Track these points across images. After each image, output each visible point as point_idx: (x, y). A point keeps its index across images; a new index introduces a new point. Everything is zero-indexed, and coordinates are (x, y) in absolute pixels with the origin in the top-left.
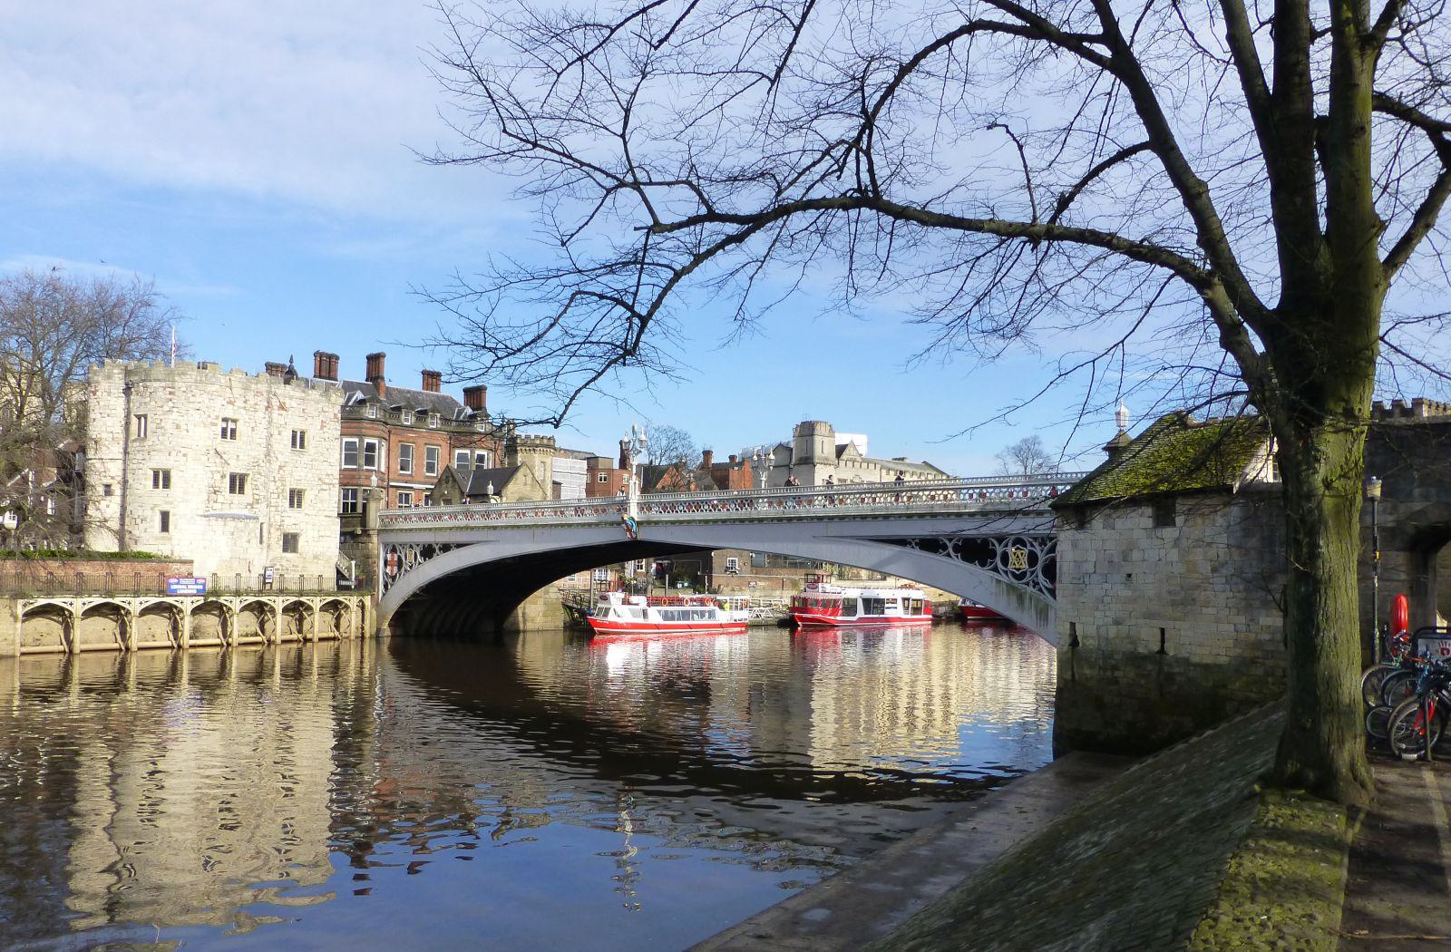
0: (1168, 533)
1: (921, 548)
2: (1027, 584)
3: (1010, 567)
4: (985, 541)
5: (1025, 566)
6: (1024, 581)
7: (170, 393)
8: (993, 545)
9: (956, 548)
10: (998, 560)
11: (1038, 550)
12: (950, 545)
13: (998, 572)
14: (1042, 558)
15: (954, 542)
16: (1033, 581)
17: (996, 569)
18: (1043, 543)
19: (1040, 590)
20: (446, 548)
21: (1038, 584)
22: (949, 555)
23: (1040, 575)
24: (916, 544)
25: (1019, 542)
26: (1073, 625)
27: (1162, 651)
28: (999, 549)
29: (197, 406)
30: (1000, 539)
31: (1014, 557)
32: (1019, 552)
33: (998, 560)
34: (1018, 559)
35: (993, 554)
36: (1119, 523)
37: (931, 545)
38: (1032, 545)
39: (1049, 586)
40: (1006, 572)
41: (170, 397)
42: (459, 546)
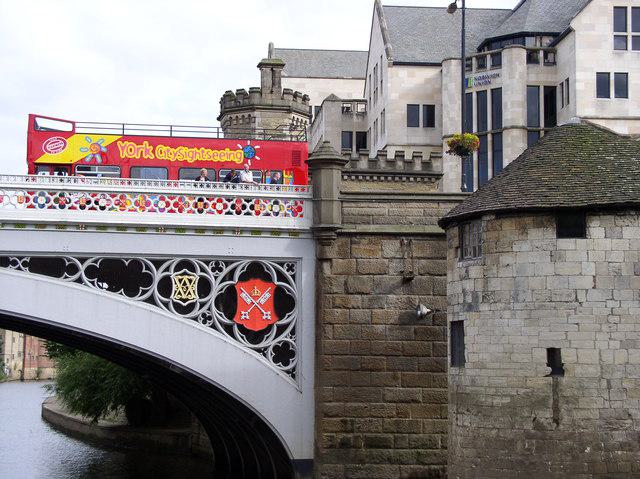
1: (31, 271)
2: (195, 319)
3: (174, 297)
4: (136, 264)
5: (195, 297)
6: (192, 314)
8: (148, 268)
9: (91, 272)
10: (155, 286)
11: (211, 276)
12: (82, 268)
13: (154, 303)
14: (217, 288)
15: (88, 263)
16: (204, 315)
17: (151, 300)
18: (217, 268)
19: (213, 326)
21: (210, 318)
22: (79, 281)
23: (214, 308)
24: (25, 264)
25: (185, 265)
26: (553, 355)
28: (158, 275)
30: (158, 264)
31: (180, 286)
32: (185, 278)
33: (155, 286)
34: (185, 287)
35: (149, 280)
36: (628, 232)
38: (203, 270)
39: (227, 321)
40: (166, 305)
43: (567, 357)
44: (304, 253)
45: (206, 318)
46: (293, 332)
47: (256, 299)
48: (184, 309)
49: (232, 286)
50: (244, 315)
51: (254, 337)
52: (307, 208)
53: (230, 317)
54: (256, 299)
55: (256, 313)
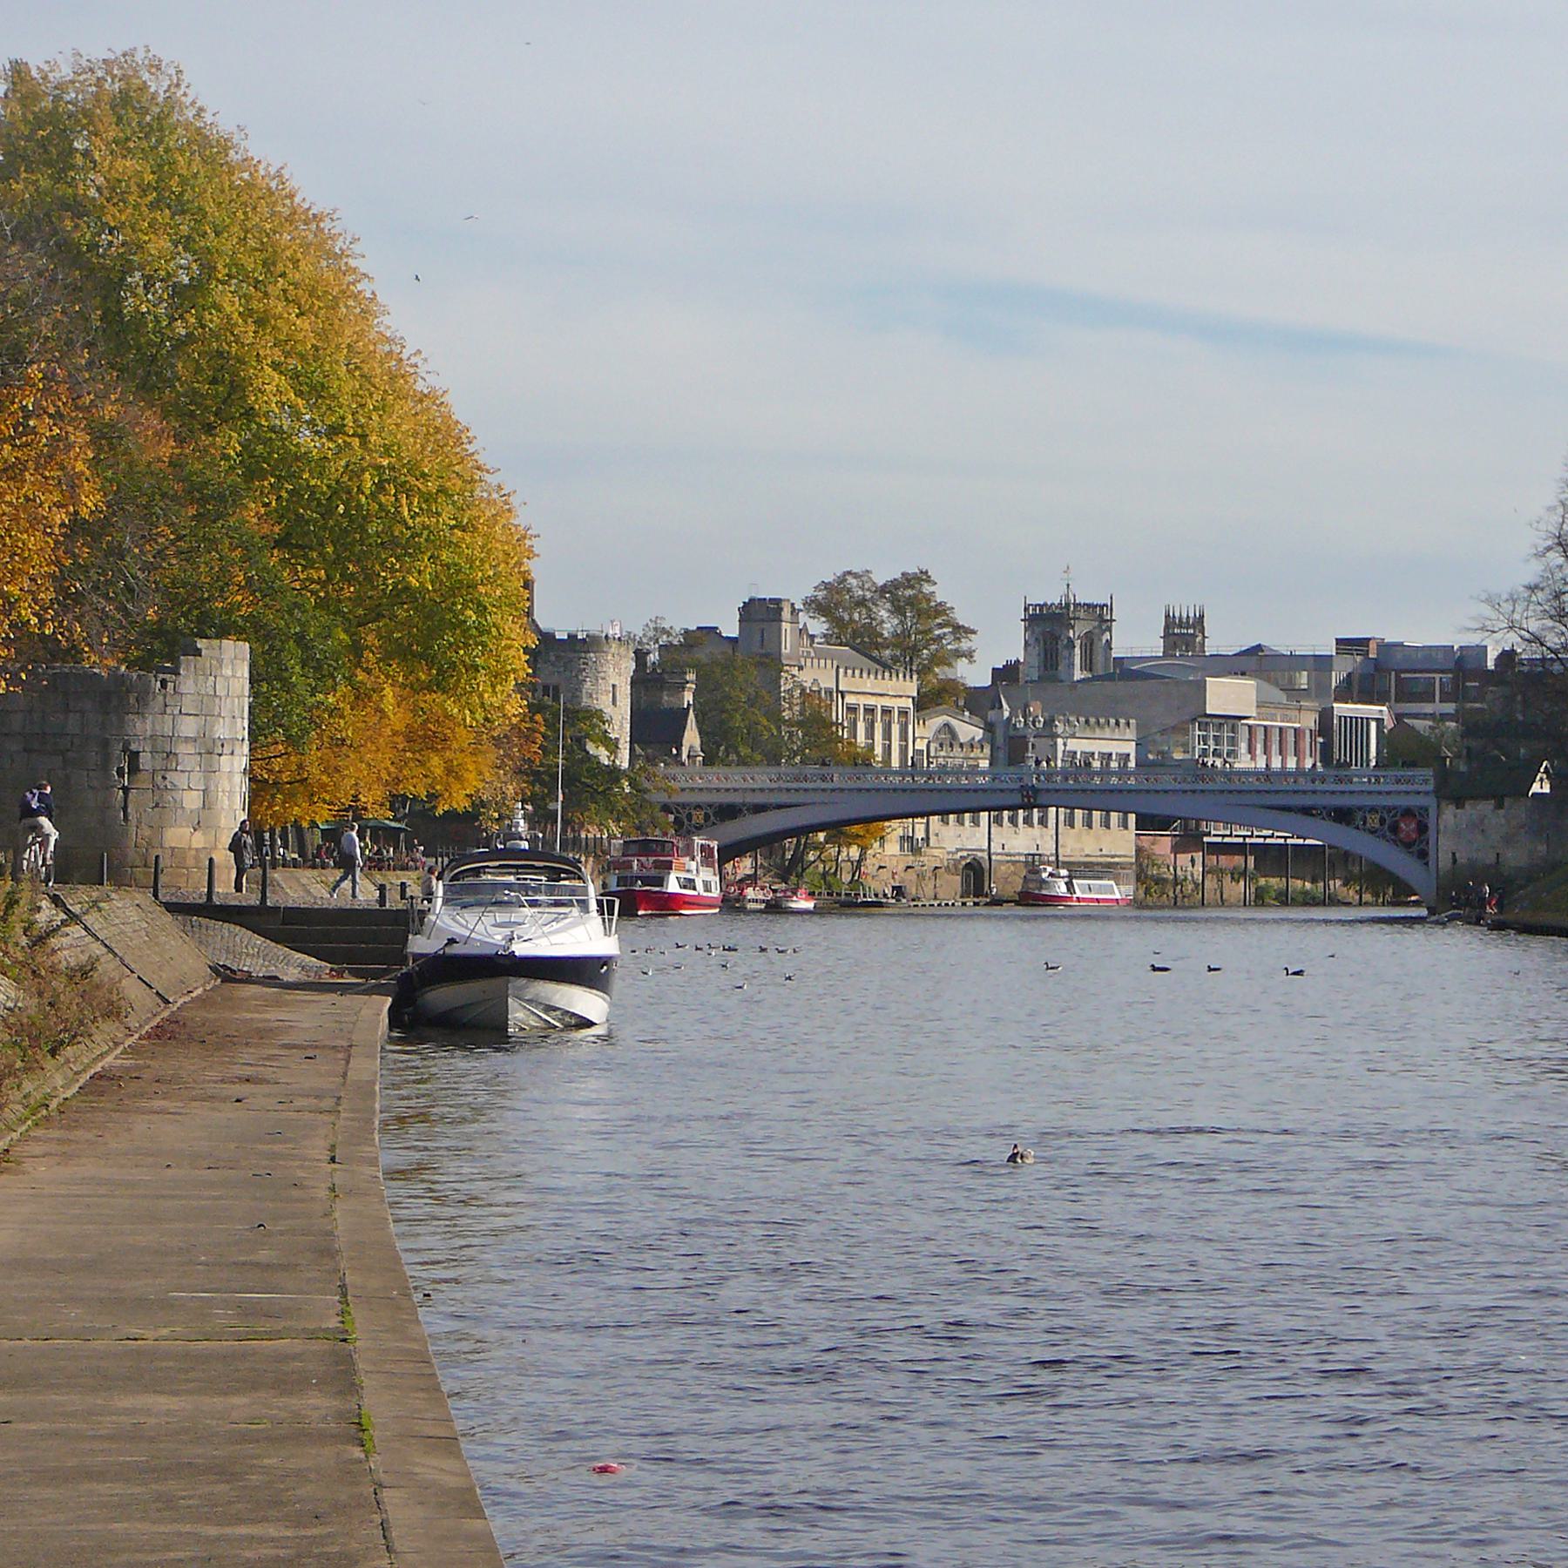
0: (1501, 812)
2: (1378, 837)
5: (1377, 826)
7: (584, 664)
17: (1357, 828)
20: (759, 809)
22: (1324, 819)
25: (1373, 810)
26: (1454, 854)
27: (1498, 862)
29: (602, 674)
30: (1360, 808)
34: (1373, 821)
37: (1306, 811)
41: (582, 666)
42: (780, 807)
43: (1457, 855)
44: (1430, 802)
45: (1384, 836)
46: (1428, 843)
47: (1408, 827)
48: (1373, 832)
49: (1397, 821)
50: (1402, 836)
51: (1408, 845)
52: (1432, 781)
53: (1395, 834)
54: (1408, 827)
55: (1408, 835)
